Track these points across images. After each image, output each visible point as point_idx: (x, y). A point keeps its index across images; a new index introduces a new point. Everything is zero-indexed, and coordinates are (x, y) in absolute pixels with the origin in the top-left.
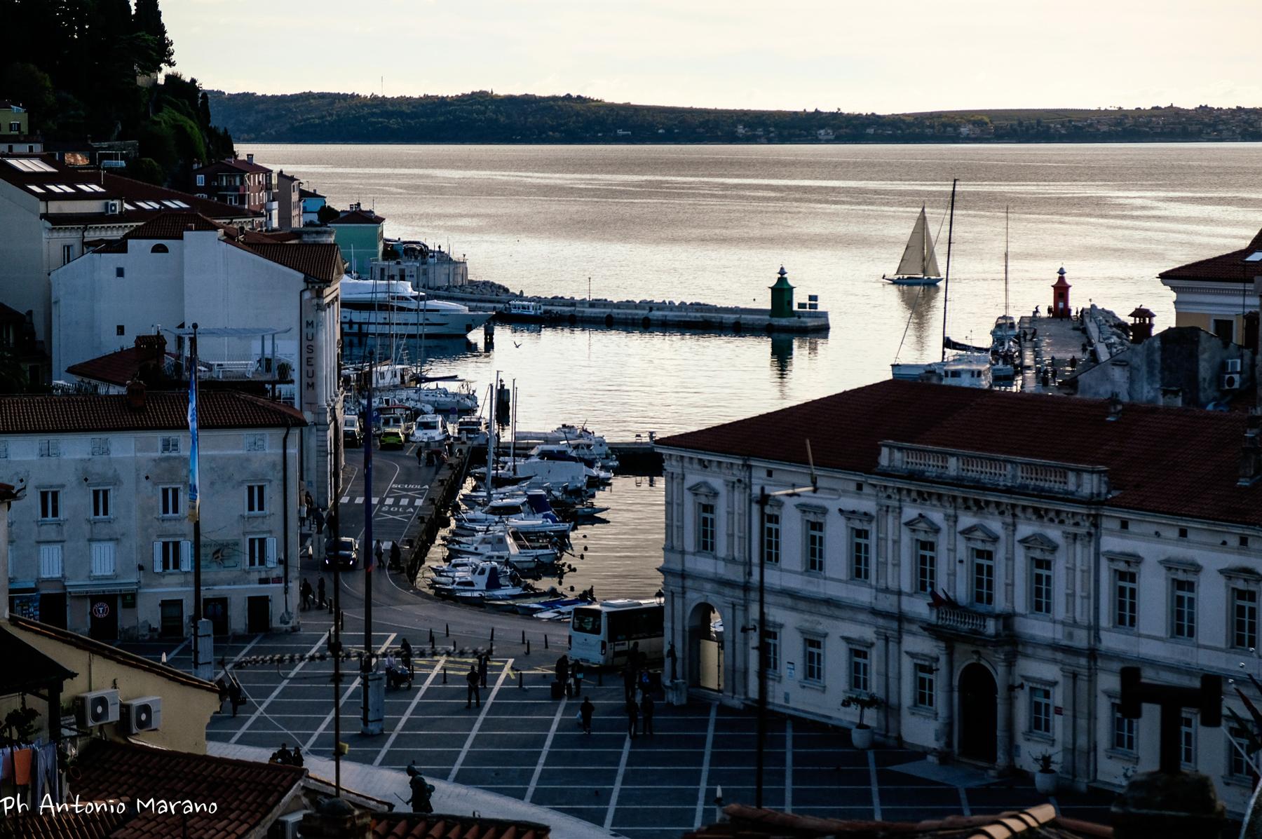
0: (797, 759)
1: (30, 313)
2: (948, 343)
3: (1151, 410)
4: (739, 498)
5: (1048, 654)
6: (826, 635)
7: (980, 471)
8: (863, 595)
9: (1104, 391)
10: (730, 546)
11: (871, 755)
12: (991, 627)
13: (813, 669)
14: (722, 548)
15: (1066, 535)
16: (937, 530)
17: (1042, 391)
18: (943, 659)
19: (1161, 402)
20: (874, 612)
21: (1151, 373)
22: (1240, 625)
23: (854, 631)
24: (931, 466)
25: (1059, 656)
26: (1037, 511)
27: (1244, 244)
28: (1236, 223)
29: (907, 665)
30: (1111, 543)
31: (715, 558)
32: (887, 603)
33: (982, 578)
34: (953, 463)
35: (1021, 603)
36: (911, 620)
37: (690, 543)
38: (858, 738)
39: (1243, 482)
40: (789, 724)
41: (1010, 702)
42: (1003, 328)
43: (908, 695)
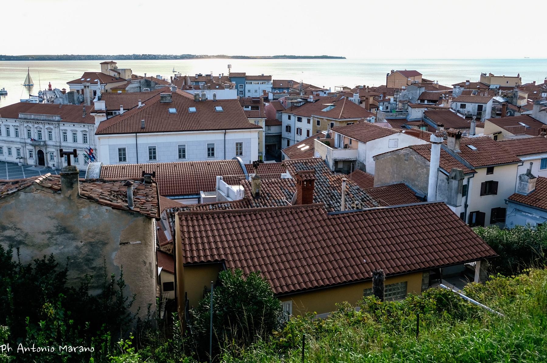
0: (8, 169)
2: (30, 95)
3: (67, 105)
7: (37, 117)
8: (18, 140)
9: (58, 103)
11: (22, 167)
12: (42, 143)
13: (10, 153)
16: (31, 128)
17: (48, 103)
18: (34, 150)
19: (68, 104)
20: (20, 143)
21: (66, 98)
22: (85, 140)
23: (17, 146)
24: (28, 117)
26: (48, 123)
27: (81, 77)
28: (80, 74)
29: (28, 151)
30: (62, 127)
32: (23, 141)
33: (40, 135)
34: (32, 116)
35: (47, 139)
36: (27, 143)
38: (19, 164)
39: (83, 116)
40: (6, 163)
41: (47, 156)
42: (40, 92)
43: (28, 156)
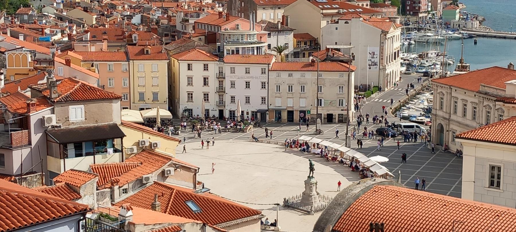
37: (438, 108)
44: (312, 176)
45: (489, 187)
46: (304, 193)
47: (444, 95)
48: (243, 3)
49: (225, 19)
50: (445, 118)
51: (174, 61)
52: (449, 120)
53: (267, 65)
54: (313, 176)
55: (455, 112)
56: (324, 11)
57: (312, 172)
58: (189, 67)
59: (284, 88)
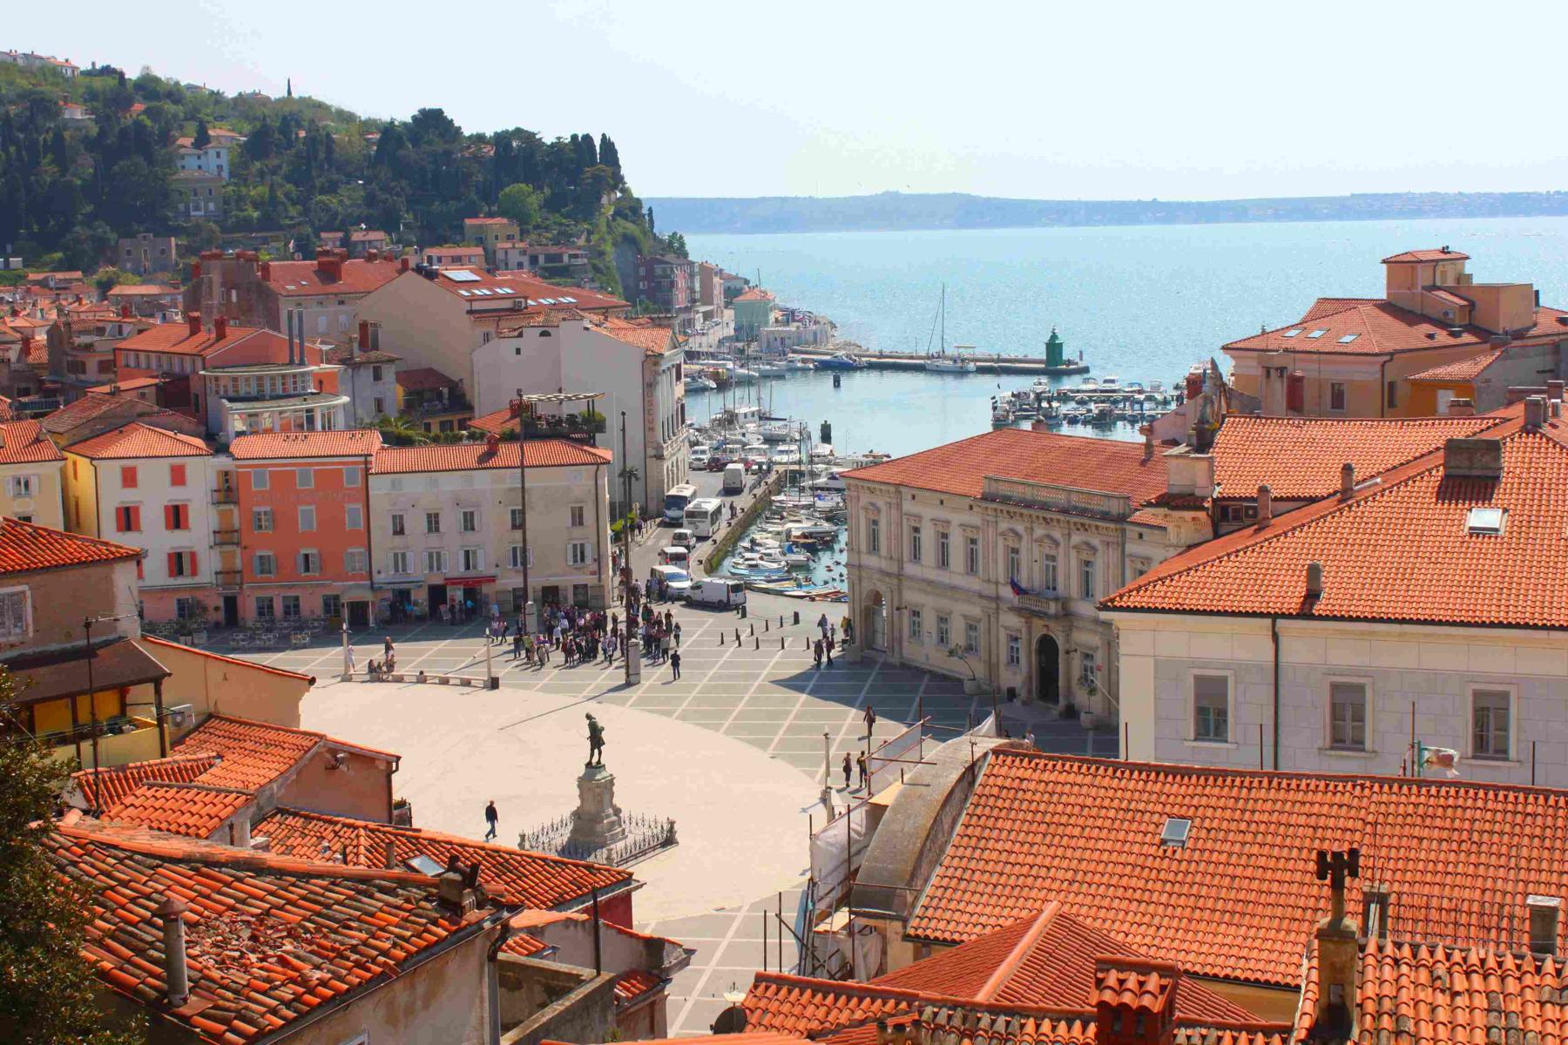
1: (461, 380)
4: (894, 512)
5: (1092, 627)
6: (951, 613)
8: (975, 584)
10: (889, 549)
12: (1053, 608)
14: (883, 551)
15: (1102, 542)
18: (1024, 631)
20: (981, 596)
25: (1100, 629)
31: (880, 556)
32: (990, 590)
35: (1075, 589)
37: (863, 547)
40: (927, 677)
44: (599, 762)
45: (1195, 740)
46: (577, 815)
47: (879, 510)
48: (234, 293)
49: (214, 336)
50: (888, 574)
51: (75, 463)
52: (899, 576)
53: (363, 459)
54: (603, 762)
55: (916, 556)
56: (477, 306)
57: (596, 751)
58: (129, 478)
59: (416, 524)
